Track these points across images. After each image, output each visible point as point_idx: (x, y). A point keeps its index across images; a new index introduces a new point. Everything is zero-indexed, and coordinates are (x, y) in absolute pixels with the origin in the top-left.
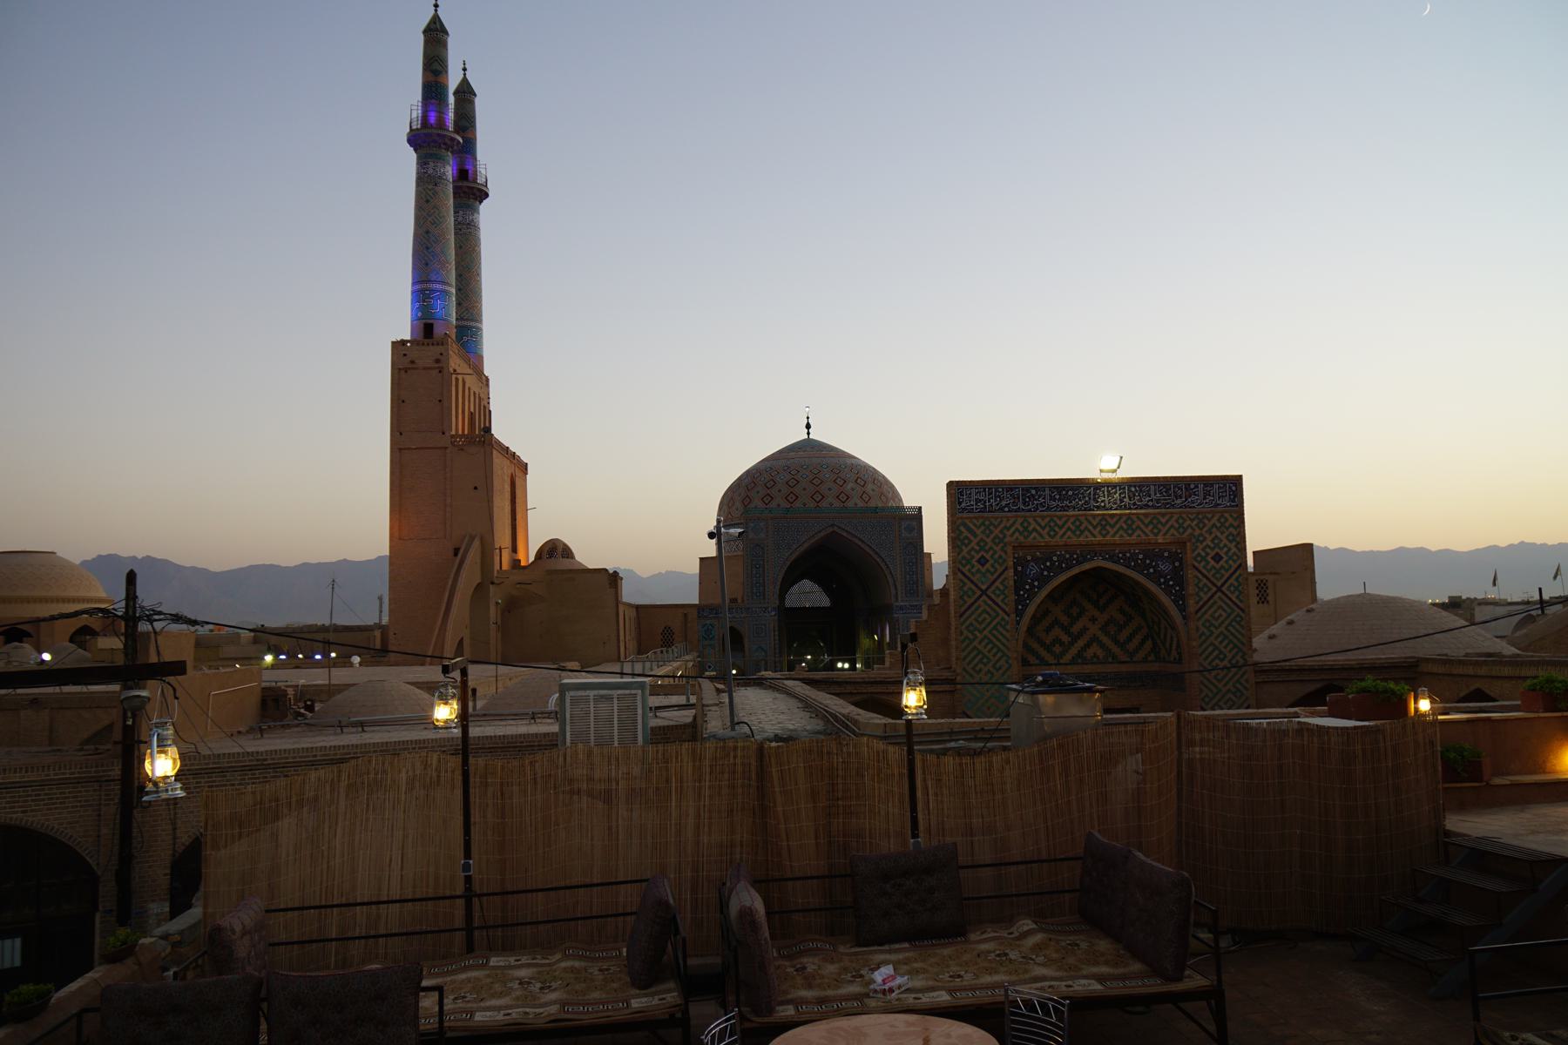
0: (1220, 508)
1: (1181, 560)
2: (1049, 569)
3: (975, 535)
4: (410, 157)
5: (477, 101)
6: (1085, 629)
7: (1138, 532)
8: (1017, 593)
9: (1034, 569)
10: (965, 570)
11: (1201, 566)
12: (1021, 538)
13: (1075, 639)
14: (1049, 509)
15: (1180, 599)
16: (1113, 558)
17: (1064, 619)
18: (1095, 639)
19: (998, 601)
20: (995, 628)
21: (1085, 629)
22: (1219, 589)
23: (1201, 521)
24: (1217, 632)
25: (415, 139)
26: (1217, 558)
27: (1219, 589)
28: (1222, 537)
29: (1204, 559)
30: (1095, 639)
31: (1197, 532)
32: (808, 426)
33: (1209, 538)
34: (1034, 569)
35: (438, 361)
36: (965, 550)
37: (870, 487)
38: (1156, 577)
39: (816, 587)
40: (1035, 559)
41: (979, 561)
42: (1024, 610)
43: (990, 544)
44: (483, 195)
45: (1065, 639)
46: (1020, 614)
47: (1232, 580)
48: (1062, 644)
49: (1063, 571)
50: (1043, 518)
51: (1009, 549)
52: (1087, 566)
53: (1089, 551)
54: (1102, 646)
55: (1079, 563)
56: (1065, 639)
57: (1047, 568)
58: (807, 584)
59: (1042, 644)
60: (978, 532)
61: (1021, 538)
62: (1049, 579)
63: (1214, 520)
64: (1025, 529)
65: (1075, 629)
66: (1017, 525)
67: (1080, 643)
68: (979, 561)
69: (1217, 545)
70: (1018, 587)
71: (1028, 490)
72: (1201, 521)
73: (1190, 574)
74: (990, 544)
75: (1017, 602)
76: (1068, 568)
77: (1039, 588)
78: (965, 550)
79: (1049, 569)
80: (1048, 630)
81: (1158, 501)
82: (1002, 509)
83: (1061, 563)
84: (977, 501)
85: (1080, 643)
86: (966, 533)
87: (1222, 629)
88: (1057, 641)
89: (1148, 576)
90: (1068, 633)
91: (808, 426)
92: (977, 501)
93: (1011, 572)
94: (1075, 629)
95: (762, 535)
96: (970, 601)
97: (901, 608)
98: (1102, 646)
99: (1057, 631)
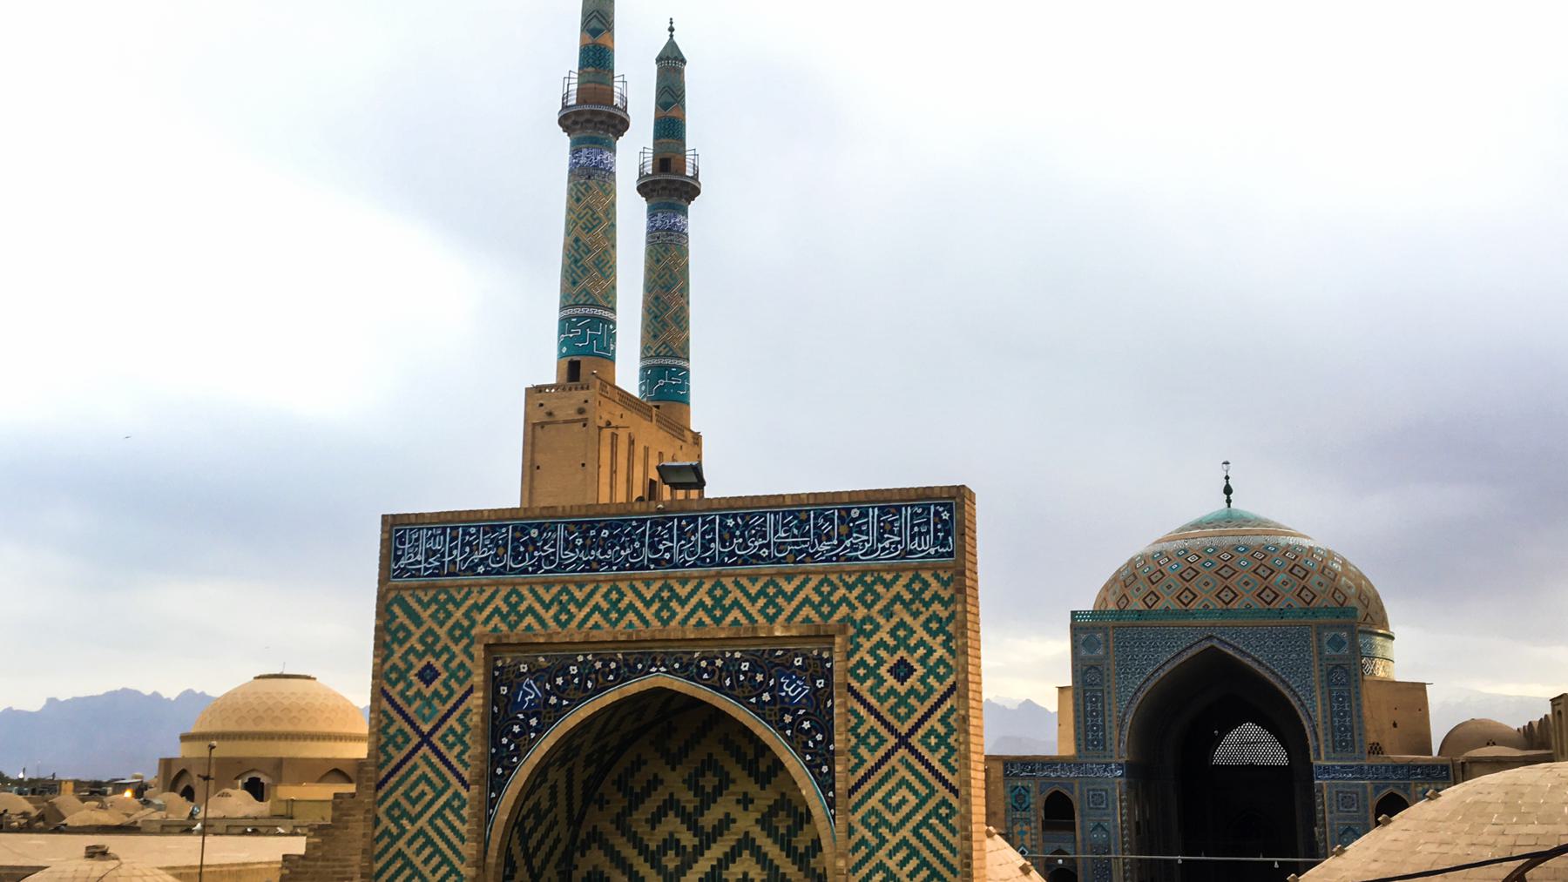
0: (914, 560)
1: (828, 675)
2: (559, 692)
3: (418, 622)
4: (562, 142)
5: (687, 69)
6: (727, 821)
7: (736, 614)
8: (496, 742)
9: (531, 692)
10: (394, 693)
11: (864, 689)
12: (504, 628)
13: (707, 840)
14: (562, 567)
15: (821, 760)
16: (689, 671)
17: (688, 799)
18: (746, 843)
19: (451, 757)
20: (439, 814)
21: (727, 821)
22: (903, 741)
23: (869, 588)
24: (893, 840)
25: (569, 120)
26: (902, 671)
27: (903, 741)
28: (916, 624)
29: (872, 672)
30: (746, 843)
31: (861, 613)
32: (1228, 490)
33: (886, 626)
34: (531, 692)
35: (581, 411)
36: (399, 651)
37: (1314, 579)
38: (774, 712)
39: (1265, 735)
40: (536, 673)
41: (421, 675)
42: (505, 778)
43: (445, 639)
44: (691, 190)
45: (688, 839)
46: (497, 785)
47: (934, 721)
48: (680, 849)
49: (589, 695)
50: (548, 585)
51: (478, 651)
52: (634, 687)
53: (638, 656)
54: (761, 858)
55: (621, 679)
56: (688, 839)
57: (557, 691)
58: (1250, 730)
59: (643, 850)
60: (425, 615)
61: (504, 628)
62: (559, 712)
63: (899, 587)
64: (513, 607)
65: (710, 819)
66: (498, 602)
67: (717, 851)
68: (421, 675)
69: (902, 642)
70: (496, 726)
71: (524, 530)
72: (869, 588)
73: (839, 705)
74: (445, 639)
75: (495, 760)
76: (599, 690)
77: (540, 730)
78: (399, 651)
79: (559, 692)
80: (654, 821)
81: (780, 547)
82: (472, 569)
83: (584, 678)
84: (430, 553)
85: (717, 851)
86: (402, 618)
87: (906, 832)
88: (672, 843)
89: (759, 709)
90: (694, 828)
91: (1228, 490)
92: (430, 553)
93: (477, 700)
94: (710, 819)
95: (1100, 652)
96: (398, 757)
97: (1327, 770)
98: (761, 858)
99: (671, 824)
